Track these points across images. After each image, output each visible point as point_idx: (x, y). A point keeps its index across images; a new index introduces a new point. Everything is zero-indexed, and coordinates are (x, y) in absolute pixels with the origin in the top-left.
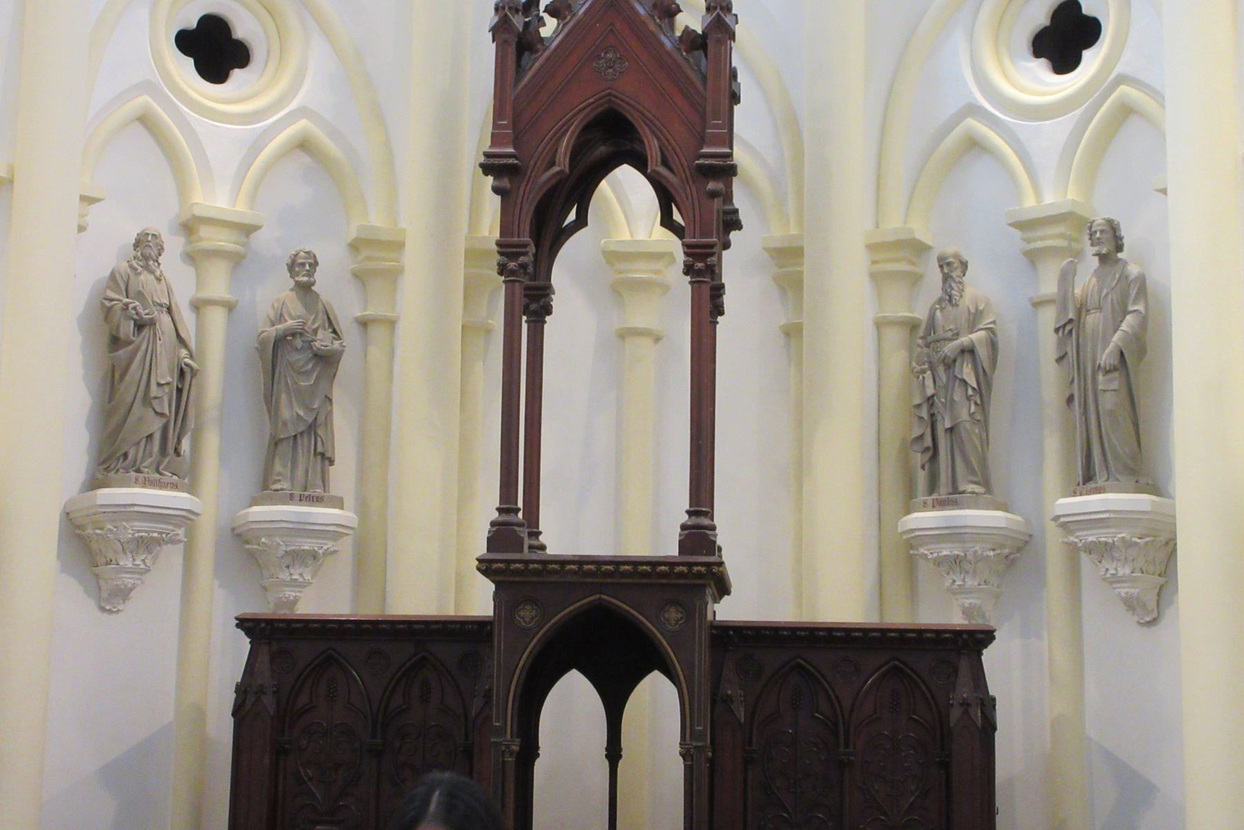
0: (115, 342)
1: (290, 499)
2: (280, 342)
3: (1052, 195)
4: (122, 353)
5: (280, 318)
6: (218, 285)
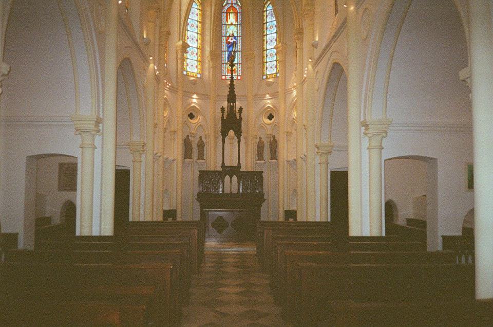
3: (269, 132)
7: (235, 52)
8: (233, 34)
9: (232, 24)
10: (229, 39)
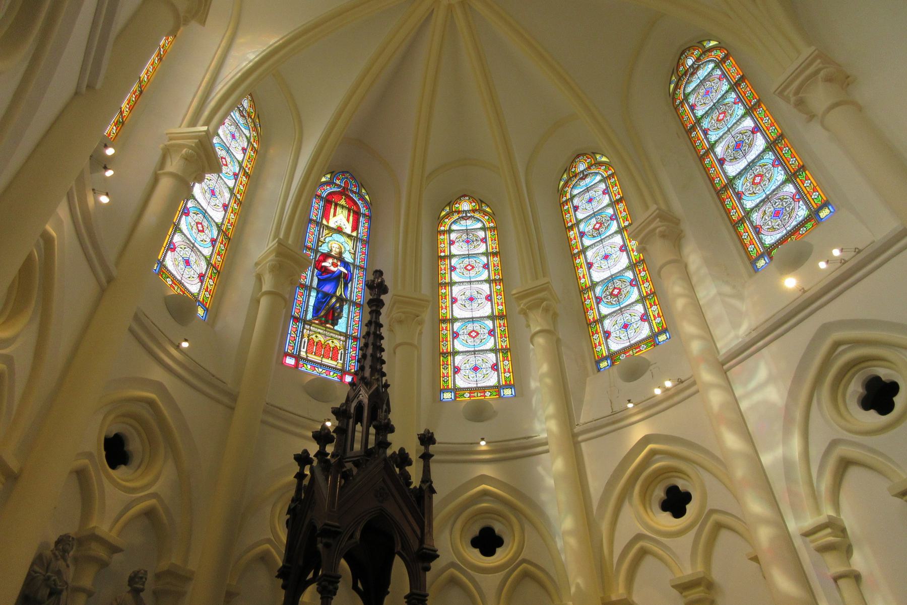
7: (341, 300)
8: (340, 253)
9: (339, 230)
10: (325, 261)
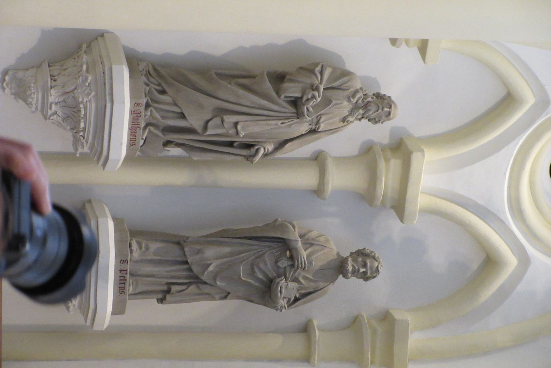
0: (279, 78)
1: (122, 260)
2: (284, 245)
4: (268, 86)
5: (308, 244)
6: (339, 179)
